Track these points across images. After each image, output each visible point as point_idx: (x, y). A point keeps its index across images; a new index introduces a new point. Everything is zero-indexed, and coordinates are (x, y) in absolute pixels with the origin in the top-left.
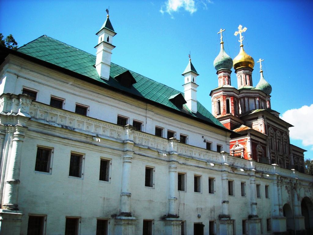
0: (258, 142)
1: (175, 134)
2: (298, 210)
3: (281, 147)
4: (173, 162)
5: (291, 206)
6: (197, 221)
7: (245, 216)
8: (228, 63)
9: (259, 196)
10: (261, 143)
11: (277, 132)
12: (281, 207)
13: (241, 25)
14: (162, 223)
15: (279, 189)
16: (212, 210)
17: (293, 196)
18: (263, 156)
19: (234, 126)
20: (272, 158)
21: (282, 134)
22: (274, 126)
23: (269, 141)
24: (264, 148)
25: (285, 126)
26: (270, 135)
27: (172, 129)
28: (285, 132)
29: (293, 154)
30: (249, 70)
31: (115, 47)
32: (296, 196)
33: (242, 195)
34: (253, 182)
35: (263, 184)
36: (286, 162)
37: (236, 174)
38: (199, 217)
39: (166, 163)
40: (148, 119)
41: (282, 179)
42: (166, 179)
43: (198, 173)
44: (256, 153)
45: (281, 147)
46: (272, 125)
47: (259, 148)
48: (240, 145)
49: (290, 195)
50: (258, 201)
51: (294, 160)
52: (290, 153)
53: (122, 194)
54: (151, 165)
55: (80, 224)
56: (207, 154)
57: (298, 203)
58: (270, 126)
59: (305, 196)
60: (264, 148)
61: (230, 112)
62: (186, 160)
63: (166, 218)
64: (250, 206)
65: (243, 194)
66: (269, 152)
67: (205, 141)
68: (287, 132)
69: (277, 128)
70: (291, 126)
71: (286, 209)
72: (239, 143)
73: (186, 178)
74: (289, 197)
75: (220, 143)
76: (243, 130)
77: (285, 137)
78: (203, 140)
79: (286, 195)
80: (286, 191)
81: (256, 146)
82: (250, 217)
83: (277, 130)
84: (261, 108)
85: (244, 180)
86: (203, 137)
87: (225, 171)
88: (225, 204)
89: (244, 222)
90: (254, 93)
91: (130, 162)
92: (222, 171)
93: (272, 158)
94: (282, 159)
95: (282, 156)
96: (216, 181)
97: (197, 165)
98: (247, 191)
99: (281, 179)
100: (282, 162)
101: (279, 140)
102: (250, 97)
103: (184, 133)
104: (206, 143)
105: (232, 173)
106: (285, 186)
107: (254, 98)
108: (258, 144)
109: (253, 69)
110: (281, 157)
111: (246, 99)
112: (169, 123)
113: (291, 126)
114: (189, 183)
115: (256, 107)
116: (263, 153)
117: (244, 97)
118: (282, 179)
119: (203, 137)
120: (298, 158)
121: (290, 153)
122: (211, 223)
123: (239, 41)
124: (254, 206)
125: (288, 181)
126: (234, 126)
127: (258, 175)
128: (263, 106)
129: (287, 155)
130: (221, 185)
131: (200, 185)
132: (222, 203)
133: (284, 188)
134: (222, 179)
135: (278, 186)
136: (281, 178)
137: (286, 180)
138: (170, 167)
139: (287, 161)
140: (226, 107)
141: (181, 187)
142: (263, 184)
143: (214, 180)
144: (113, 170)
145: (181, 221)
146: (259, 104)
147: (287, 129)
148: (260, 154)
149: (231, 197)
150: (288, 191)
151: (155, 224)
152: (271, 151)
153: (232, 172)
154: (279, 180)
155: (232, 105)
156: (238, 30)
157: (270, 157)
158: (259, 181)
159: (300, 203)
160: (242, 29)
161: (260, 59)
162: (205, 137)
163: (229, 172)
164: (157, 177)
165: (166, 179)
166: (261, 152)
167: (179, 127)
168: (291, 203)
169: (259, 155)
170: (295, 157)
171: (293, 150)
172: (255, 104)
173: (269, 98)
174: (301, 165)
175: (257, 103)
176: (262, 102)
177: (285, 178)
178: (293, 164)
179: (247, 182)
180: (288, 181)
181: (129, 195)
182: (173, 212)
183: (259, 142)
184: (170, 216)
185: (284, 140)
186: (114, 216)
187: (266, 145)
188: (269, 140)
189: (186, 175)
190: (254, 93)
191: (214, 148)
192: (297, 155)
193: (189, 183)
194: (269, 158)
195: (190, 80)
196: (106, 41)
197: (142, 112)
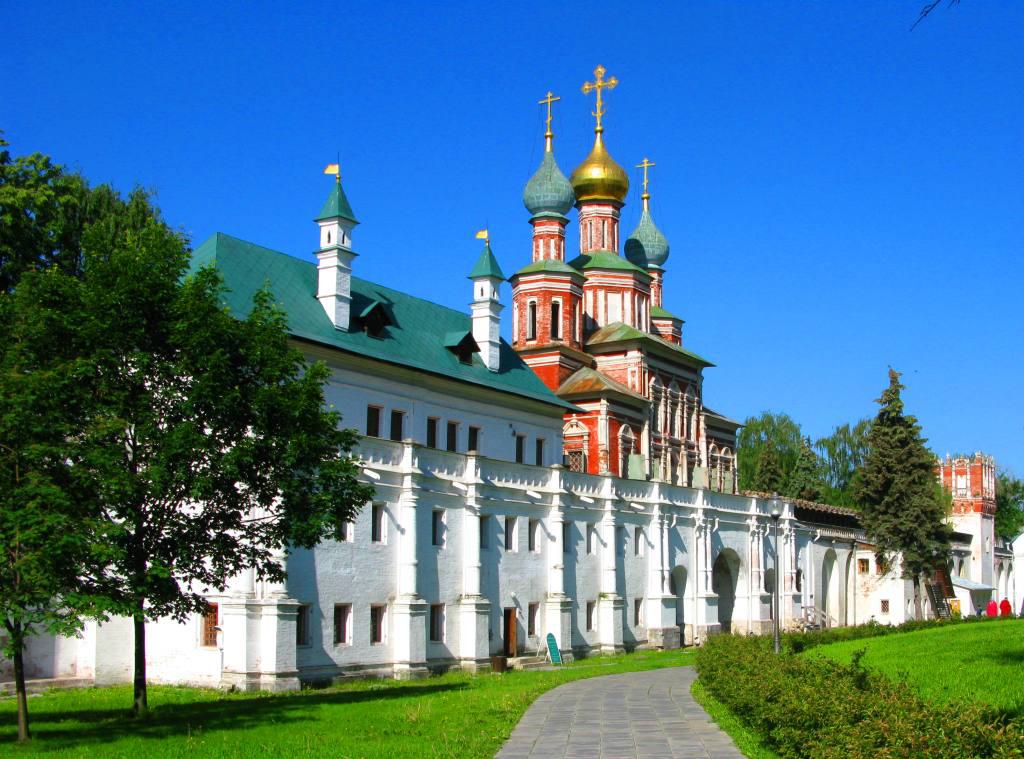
13: (603, 66)
22: (666, 372)
25: (694, 366)
28: (693, 381)
48: (580, 423)
55: (310, 615)
61: (560, 335)
67: (514, 434)
68: (696, 382)
69: (672, 374)
70: (708, 365)
72: (579, 420)
76: (592, 390)
78: (511, 431)
86: (511, 426)
103: (474, 422)
104: (515, 439)
113: (708, 365)
119: (511, 426)
123: (593, 114)
140: (550, 322)
155: (565, 318)
156: (593, 80)
160: (605, 78)
161: (645, 161)
162: (515, 424)
183: (626, 416)
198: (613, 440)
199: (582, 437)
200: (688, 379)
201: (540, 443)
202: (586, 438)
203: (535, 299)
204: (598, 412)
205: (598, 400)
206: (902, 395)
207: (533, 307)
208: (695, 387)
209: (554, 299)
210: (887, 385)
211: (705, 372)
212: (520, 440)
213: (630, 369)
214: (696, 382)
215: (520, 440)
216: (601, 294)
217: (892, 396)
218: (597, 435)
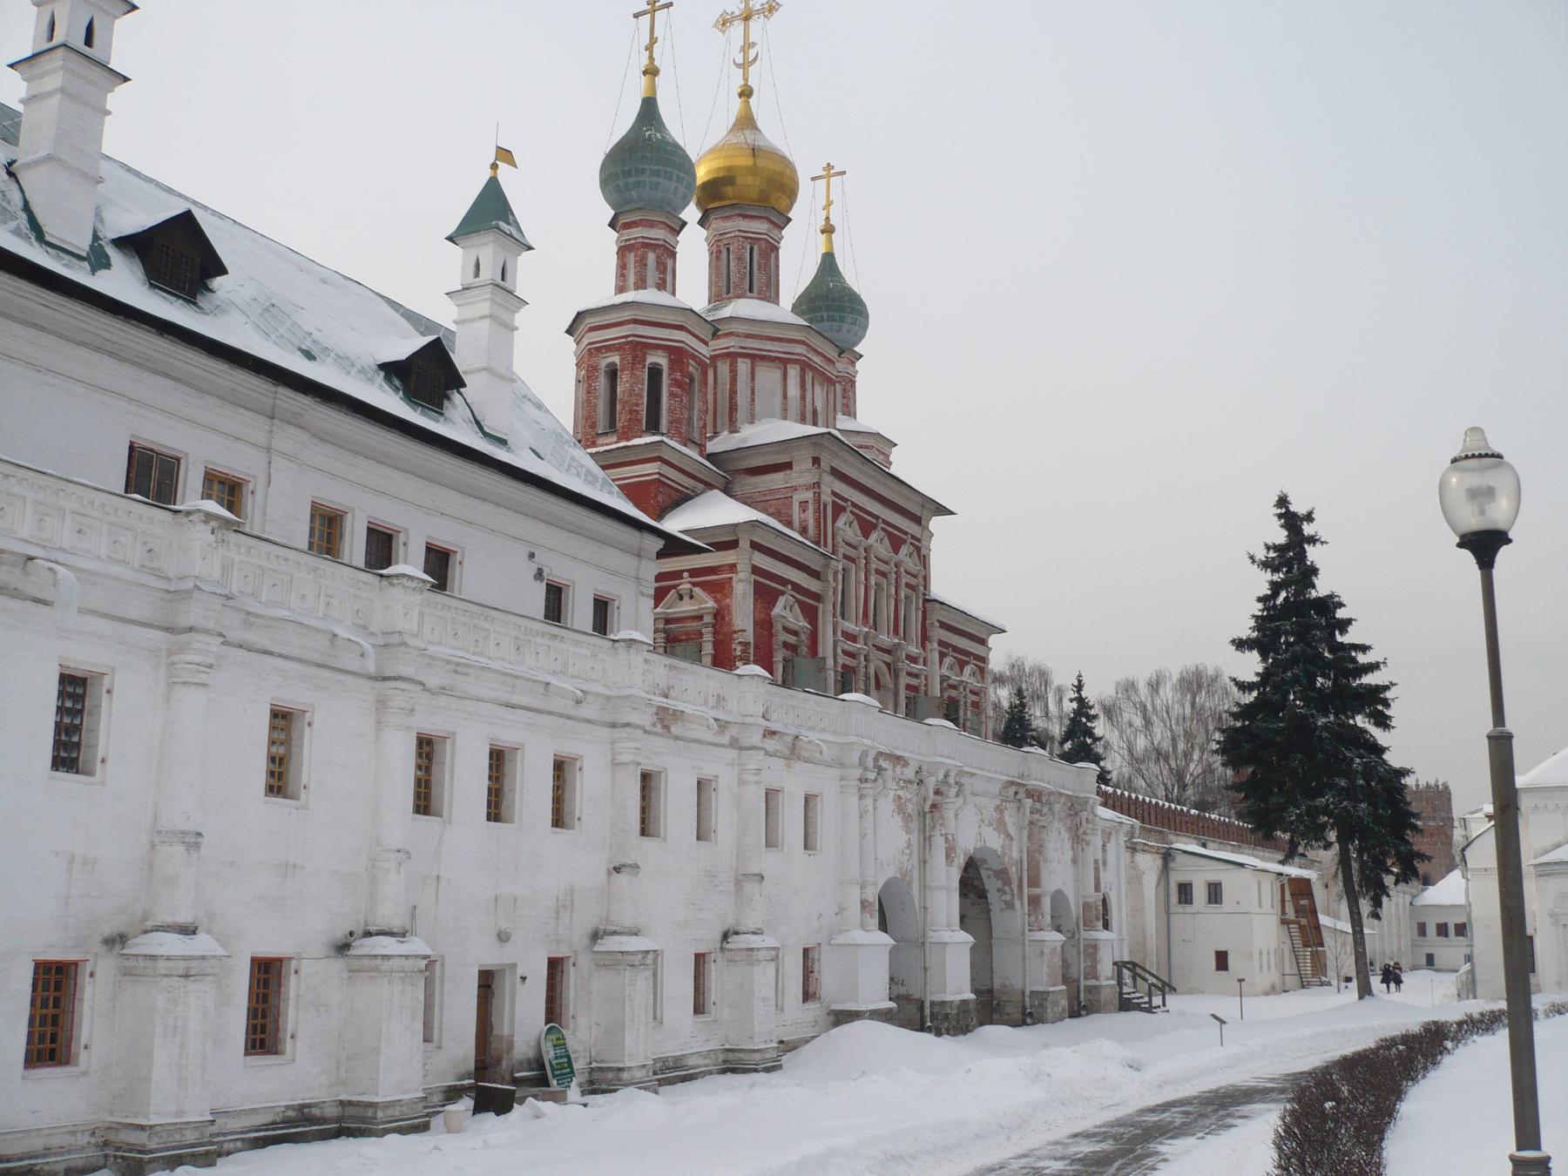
1: (402, 538)
2: (946, 903)
3: (886, 610)
4: (400, 684)
6: (491, 957)
7: (707, 940)
8: (670, 179)
10: (797, 587)
11: (874, 536)
12: (872, 895)
14: (338, 965)
15: (866, 812)
16: (565, 904)
17: (926, 840)
18: (804, 650)
20: (842, 659)
21: (896, 550)
23: (835, 580)
24: (811, 614)
25: (915, 510)
26: (841, 550)
27: (389, 516)
28: (913, 537)
29: (941, 643)
30: (771, 222)
31: (126, 79)
32: (939, 843)
33: (698, 838)
34: (752, 778)
36: (904, 680)
37: (677, 738)
38: (503, 937)
39: (366, 685)
40: (278, 461)
41: (884, 764)
42: (359, 759)
43: (507, 736)
44: (771, 635)
45: (886, 610)
46: (854, 505)
47: (785, 611)
48: (697, 590)
49: (915, 838)
50: (768, 862)
51: (944, 678)
52: (925, 638)
53: (159, 836)
54: (291, 697)
56: (552, 643)
57: (947, 878)
58: (843, 509)
59: (979, 845)
60: (811, 614)
62: (456, 672)
64: (730, 887)
66: (830, 631)
67: (539, 575)
69: (877, 518)
70: (942, 511)
73: (453, 757)
74: (909, 846)
75: (607, 589)
78: (533, 568)
79: (892, 842)
80: (898, 820)
81: (773, 603)
83: (874, 527)
84: (809, 416)
85: (708, 771)
86: (532, 555)
87: (628, 725)
88: (623, 878)
89: (700, 959)
90: (780, 340)
91: (204, 685)
92: (613, 725)
93: (842, 659)
94: (888, 665)
95: (889, 652)
96: (585, 770)
97: (506, 697)
98: (724, 817)
100: (887, 680)
101: (881, 579)
102: (763, 358)
104: (540, 590)
105: (659, 735)
106: (892, 793)
107: (784, 363)
108: (783, 593)
109: (790, 220)
110: (887, 658)
111: (743, 366)
112: (377, 487)
113: (942, 511)
114: (465, 780)
116: (803, 637)
117: (732, 357)
118: (884, 764)
119: (532, 555)
121: (925, 638)
122: (555, 965)
124: (751, 888)
127: (771, 744)
128: (819, 409)
130: (603, 792)
131: (513, 790)
132: (609, 873)
133: (887, 805)
134: (615, 764)
135: (861, 797)
136: (876, 760)
137: (898, 769)
138: (382, 704)
139: (910, 674)
141: (424, 802)
142: (794, 782)
143: (578, 764)
144: (115, 726)
145: (425, 957)
146: (803, 398)
148: (792, 639)
150: (907, 818)
151: (303, 973)
153: (658, 729)
154: (866, 769)
155: (672, 395)
157: (835, 656)
158: (777, 773)
159: (955, 875)
163: (646, 732)
164: (316, 754)
165: (359, 759)
166: (795, 633)
167: (418, 503)
168: (916, 873)
169: (786, 645)
170: (948, 661)
171: (944, 626)
172: (785, 396)
173: (853, 364)
174: (975, 698)
175: (793, 390)
176: (818, 389)
177: (897, 760)
178: (936, 691)
180: (909, 773)
181: (193, 841)
185: (905, 579)
186: (117, 941)
187: (818, 597)
188: (836, 573)
189: (453, 744)
190: (780, 340)
191: (580, 611)
192: (955, 649)
193: (465, 780)
194: (830, 662)
195: (488, 273)
196: (79, 43)
197: (254, 427)
198: (764, 625)
199: (700, 618)
200: (906, 533)
202: (708, 619)
203: (616, 359)
204: (732, 568)
205: (733, 545)
206: (1313, 554)
207: (613, 373)
208: (918, 549)
209: (651, 359)
210: (1281, 537)
211: (936, 524)
213: (798, 497)
214: (919, 540)
216: (743, 366)
217: (1291, 558)
218: (729, 612)
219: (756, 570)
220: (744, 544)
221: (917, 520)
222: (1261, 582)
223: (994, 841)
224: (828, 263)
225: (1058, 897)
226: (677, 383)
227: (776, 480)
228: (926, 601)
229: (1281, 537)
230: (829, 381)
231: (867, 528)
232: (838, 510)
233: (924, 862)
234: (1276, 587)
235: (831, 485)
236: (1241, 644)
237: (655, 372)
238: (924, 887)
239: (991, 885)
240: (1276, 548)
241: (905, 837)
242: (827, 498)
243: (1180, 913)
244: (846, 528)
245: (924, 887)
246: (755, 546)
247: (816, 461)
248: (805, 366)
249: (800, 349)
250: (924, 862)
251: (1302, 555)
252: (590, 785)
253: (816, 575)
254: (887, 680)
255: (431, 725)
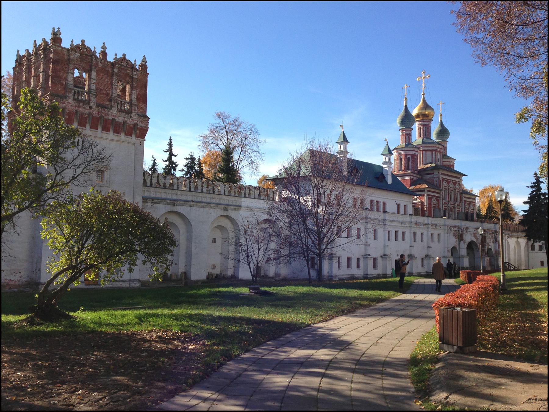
0: (433, 196)
2: (463, 251)
3: (453, 196)
5: (458, 248)
7: (424, 256)
9: (432, 241)
10: (435, 196)
12: (450, 249)
19: (413, 183)
24: (438, 200)
25: (458, 176)
27: (378, 199)
35: (436, 232)
36: (457, 209)
43: (397, 230)
45: (453, 196)
47: (434, 201)
51: (465, 207)
52: (461, 200)
60: (438, 200)
63: (384, 256)
65: (422, 241)
70: (465, 175)
71: (453, 251)
75: (406, 203)
77: (457, 187)
79: (453, 241)
82: (427, 256)
85: (423, 231)
89: (422, 259)
99: (450, 228)
100: (453, 210)
103: (385, 201)
107: (432, 151)
113: (465, 175)
115: (432, 160)
120: (469, 205)
121: (461, 200)
125: (456, 229)
126: (413, 183)
129: (458, 203)
133: (452, 235)
142: (436, 232)
147: (459, 178)
149: (415, 243)
152: (444, 201)
158: (432, 231)
159: (466, 246)
175: (434, 156)
179: (425, 233)
182: (386, 253)
184: (384, 255)
187: (439, 197)
198: (430, 204)
201: (405, 206)
205: (424, 191)
212: (399, 206)
215: (399, 206)
216: (424, 152)
219: (428, 195)
220: (426, 191)
221: (459, 178)
222: (530, 190)
223: (474, 239)
224: (441, 123)
225: (490, 250)
226: (413, 161)
227: (431, 176)
228: (461, 193)
229: (535, 181)
230: (440, 152)
231: (448, 182)
232: (443, 181)
233: (459, 244)
234: (533, 192)
235: (441, 177)
236: (525, 203)
237: (409, 159)
238: (459, 248)
239: (474, 248)
240: (534, 183)
241: (455, 240)
242: (441, 179)
243: (532, 254)
244: (445, 184)
245: (459, 248)
246: (428, 191)
247: (439, 173)
248: (436, 151)
249: (435, 148)
250: (459, 244)
251: (539, 185)
252: (407, 235)
253: (439, 193)
254: (453, 210)
255: (389, 229)
